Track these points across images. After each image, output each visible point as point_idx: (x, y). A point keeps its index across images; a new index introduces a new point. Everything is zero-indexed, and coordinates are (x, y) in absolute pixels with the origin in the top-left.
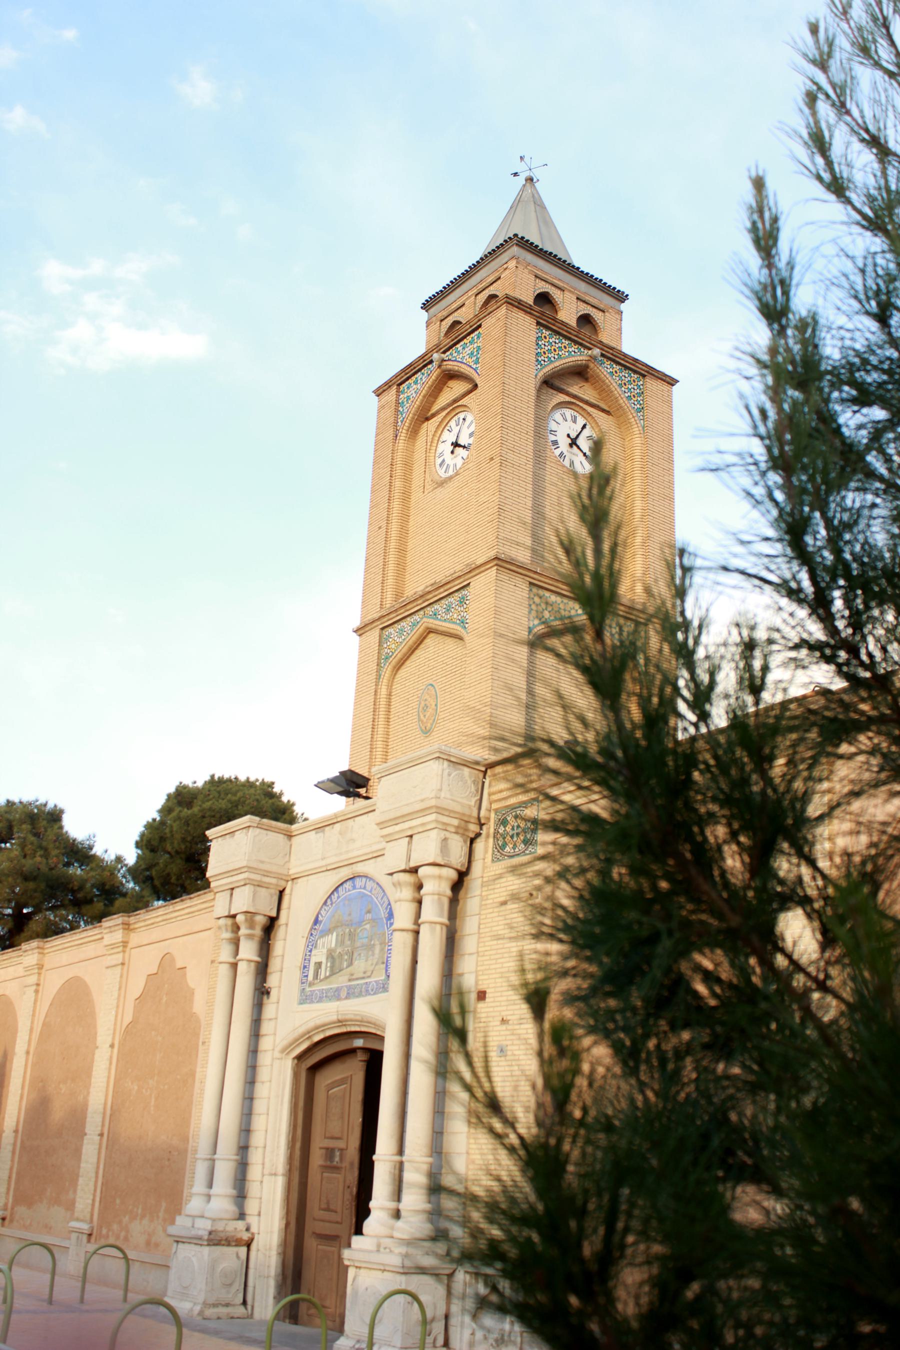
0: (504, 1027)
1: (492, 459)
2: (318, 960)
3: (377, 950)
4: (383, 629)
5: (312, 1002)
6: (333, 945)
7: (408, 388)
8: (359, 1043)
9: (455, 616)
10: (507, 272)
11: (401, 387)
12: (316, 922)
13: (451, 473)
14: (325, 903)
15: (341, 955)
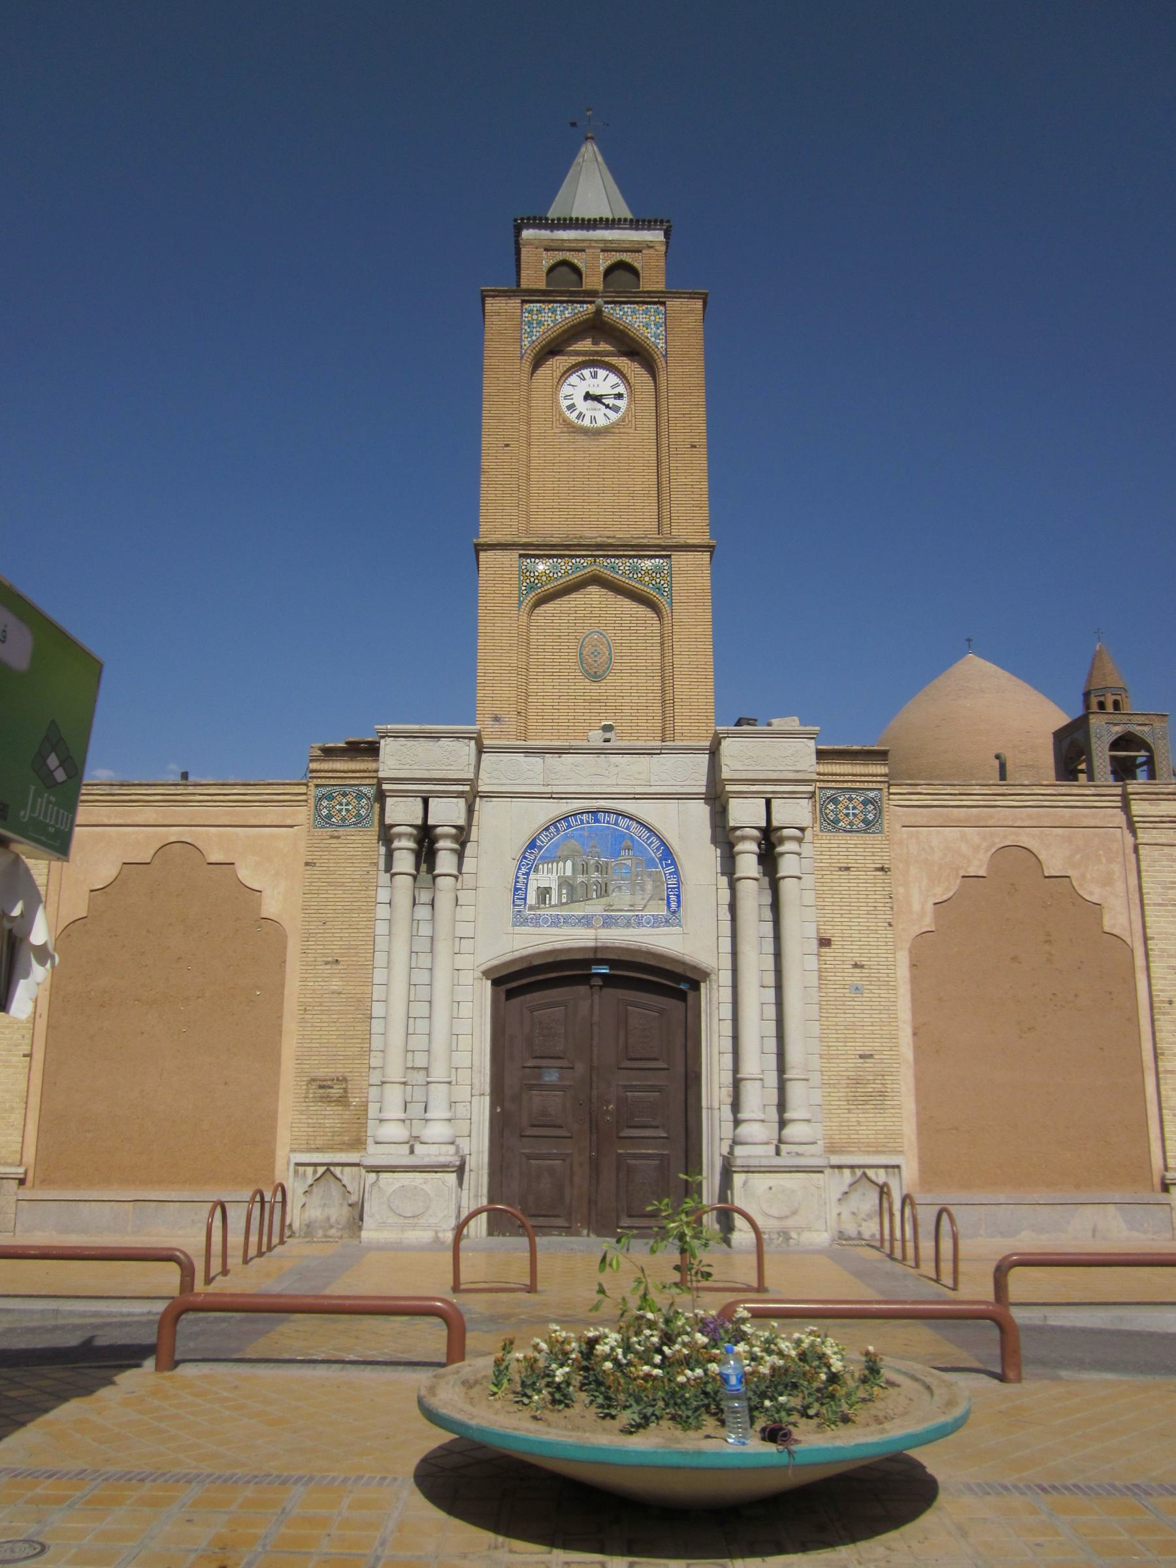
0: (858, 970)
1: (694, 447)
2: (544, 884)
3: (649, 886)
4: (521, 556)
5: (537, 925)
6: (569, 872)
7: (539, 311)
8: (605, 970)
9: (647, 579)
10: (651, 251)
11: (526, 306)
12: (532, 845)
13: (586, 422)
14: (547, 829)
15: (586, 886)
